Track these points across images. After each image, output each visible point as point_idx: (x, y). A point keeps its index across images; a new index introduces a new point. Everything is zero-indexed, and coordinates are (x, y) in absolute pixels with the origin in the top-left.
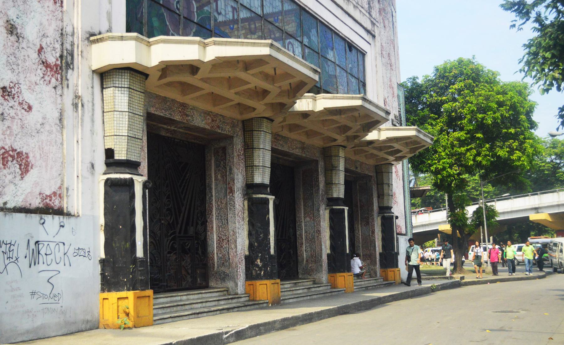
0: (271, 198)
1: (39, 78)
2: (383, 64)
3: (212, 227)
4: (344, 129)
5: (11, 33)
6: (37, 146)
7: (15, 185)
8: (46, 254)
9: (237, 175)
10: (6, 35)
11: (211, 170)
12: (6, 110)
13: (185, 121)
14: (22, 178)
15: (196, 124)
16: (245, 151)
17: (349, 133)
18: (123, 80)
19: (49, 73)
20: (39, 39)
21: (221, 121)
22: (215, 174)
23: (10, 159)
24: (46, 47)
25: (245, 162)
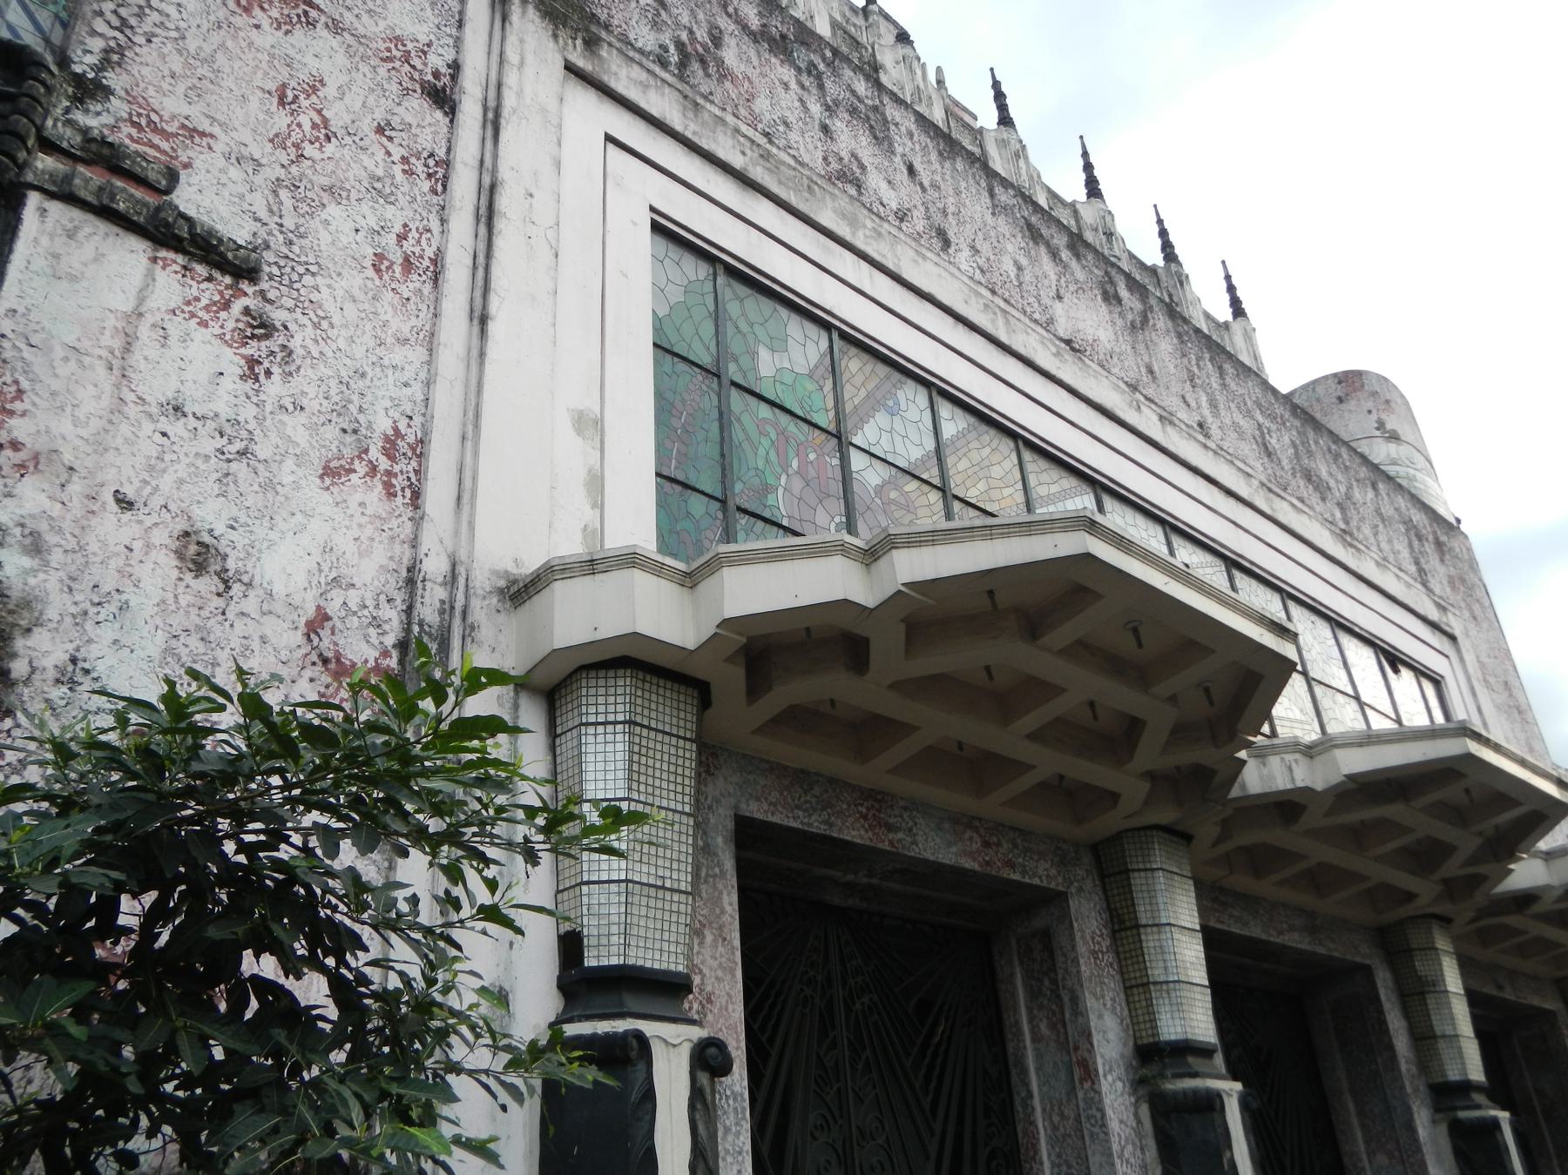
0: (1231, 1090)
2: (1498, 707)
4: (1427, 855)
5: (199, 568)
9: (1100, 1017)
10: (175, 573)
11: (1016, 1008)
13: (886, 846)
16: (1114, 939)
17: (1452, 867)
18: (611, 700)
20: (315, 592)
21: (1015, 846)
22: (1031, 1020)
24: (343, 613)
25: (1122, 974)
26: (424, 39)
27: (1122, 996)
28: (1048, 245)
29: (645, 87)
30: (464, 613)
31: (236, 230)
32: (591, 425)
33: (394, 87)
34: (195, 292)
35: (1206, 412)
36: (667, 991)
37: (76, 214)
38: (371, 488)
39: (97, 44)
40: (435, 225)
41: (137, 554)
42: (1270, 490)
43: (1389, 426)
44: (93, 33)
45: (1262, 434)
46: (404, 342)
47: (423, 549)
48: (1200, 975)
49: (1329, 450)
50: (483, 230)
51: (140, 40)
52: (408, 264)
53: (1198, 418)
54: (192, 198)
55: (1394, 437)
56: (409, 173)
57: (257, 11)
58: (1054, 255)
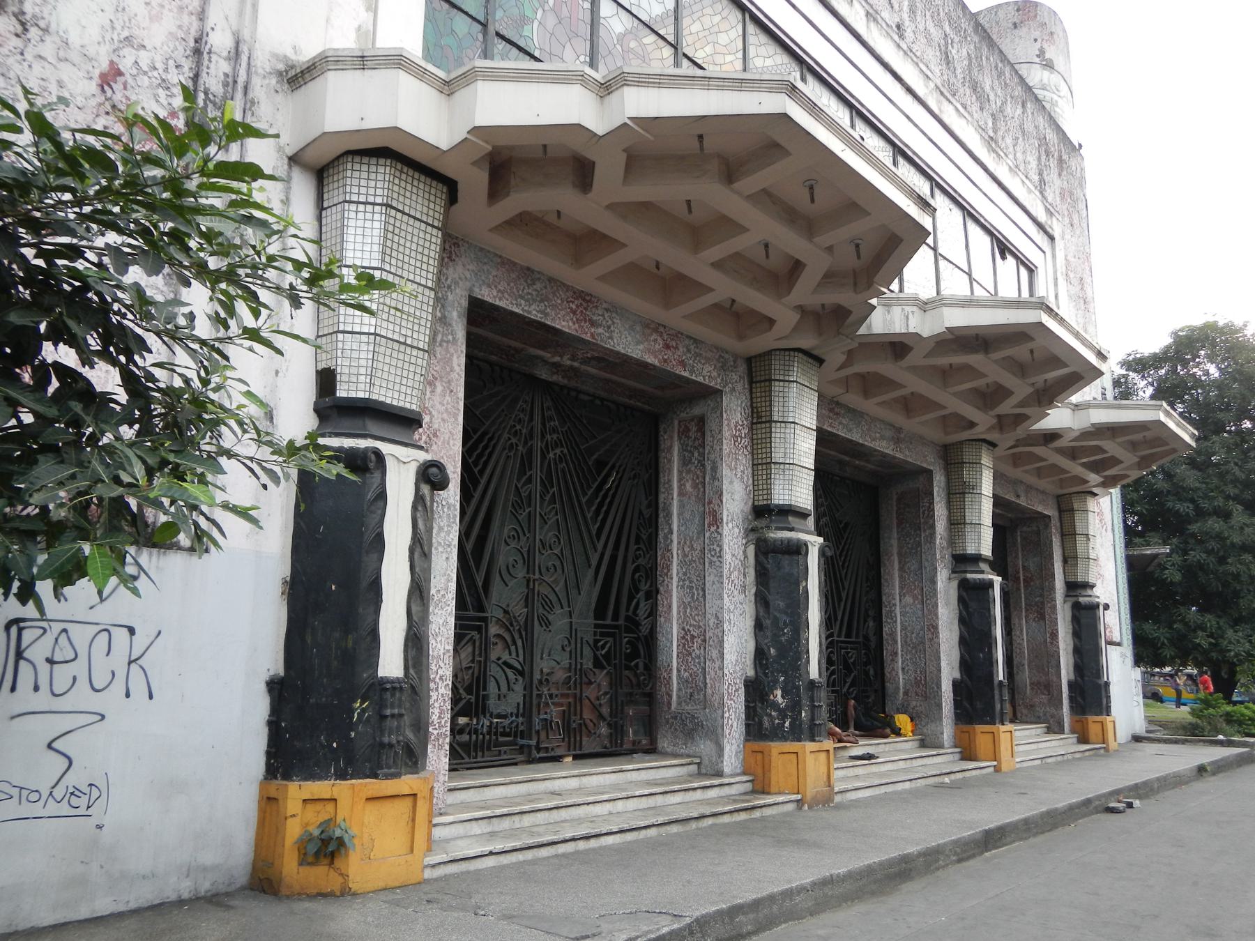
0: (815, 542)
2: (1070, 297)
3: (670, 606)
4: (990, 396)
8: (51, 661)
9: (731, 482)
11: (670, 470)
13: (588, 337)
15: (620, 349)
16: (751, 429)
17: (1006, 408)
18: (372, 184)
21: (689, 351)
22: (680, 481)
24: (135, 72)
25: (753, 454)
27: (750, 470)
30: (246, 89)
35: (906, 16)
36: (403, 422)
42: (942, 93)
43: (1047, 56)
45: (946, 43)
47: (210, 23)
48: (810, 462)
49: (996, 67)
53: (897, 20)
55: (1049, 65)
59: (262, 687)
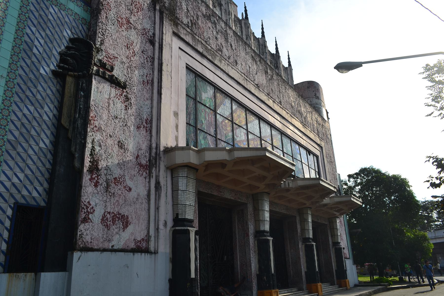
1: (136, 173)
5: (121, 148)
6: (134, 211)
7: (119, 235)
12: (116, 190)
14: (124, 231)
19: (142, 170)
20: (136, 152)
23: (117, 219)
26: (148, 28)
28: (255, 61)
29: (186, 35)
31: (122, 79)
32: (176, 114)
33: (144, 41)
34: (117, 93)
36: (190, 222)
37: (100, 78)
38: (144, 130)
39: (99, 39)
40: (151, 73)
41: (113, 146)
42: (292, 117)
44: (99, 37)
46: (147, 99)
48: (268, 219)
50: (160, 74)
51: (106, 37)
52: (148, 83)
54: (116, 73)
56: (147, 61)
57: (123, 27)
58: (256, 63)
59: (168, 281)
